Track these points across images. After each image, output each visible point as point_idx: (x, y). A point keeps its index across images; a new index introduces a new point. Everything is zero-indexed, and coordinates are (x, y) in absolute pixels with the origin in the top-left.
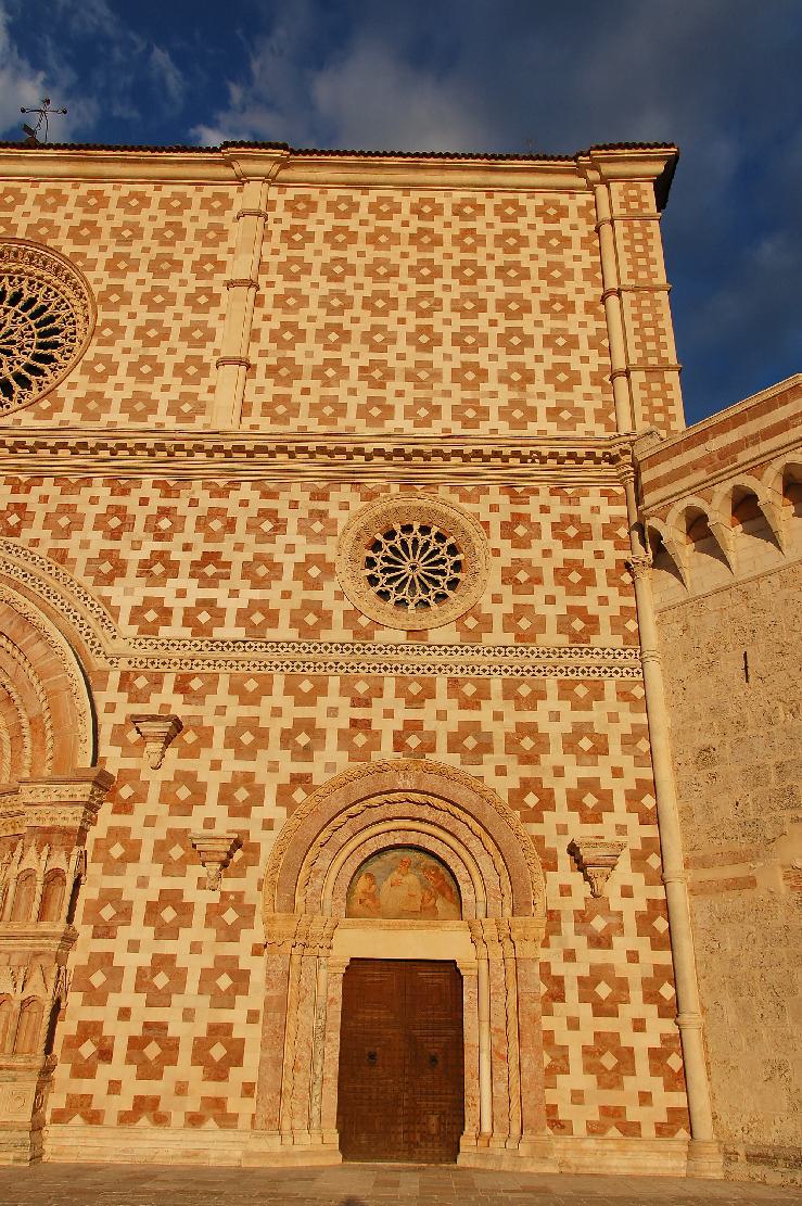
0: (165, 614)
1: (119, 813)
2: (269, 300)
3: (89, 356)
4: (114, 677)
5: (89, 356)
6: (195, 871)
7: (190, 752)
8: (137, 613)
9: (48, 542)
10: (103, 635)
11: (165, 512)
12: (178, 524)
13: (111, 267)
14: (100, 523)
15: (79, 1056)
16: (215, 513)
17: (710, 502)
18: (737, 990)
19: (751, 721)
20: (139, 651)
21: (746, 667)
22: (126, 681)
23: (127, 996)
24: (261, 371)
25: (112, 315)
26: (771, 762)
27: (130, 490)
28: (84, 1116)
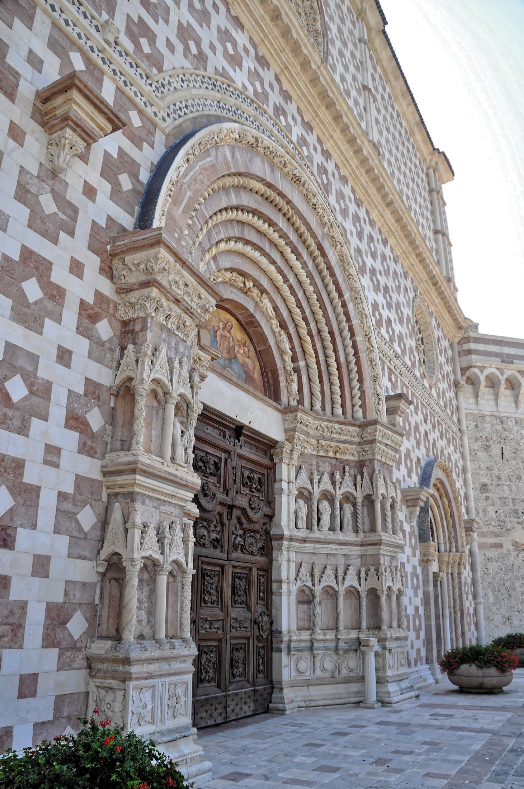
17: (502, 374)
18: (494, 590)
19: (503, 478)
21: (502, 454)
26: (510, 497)
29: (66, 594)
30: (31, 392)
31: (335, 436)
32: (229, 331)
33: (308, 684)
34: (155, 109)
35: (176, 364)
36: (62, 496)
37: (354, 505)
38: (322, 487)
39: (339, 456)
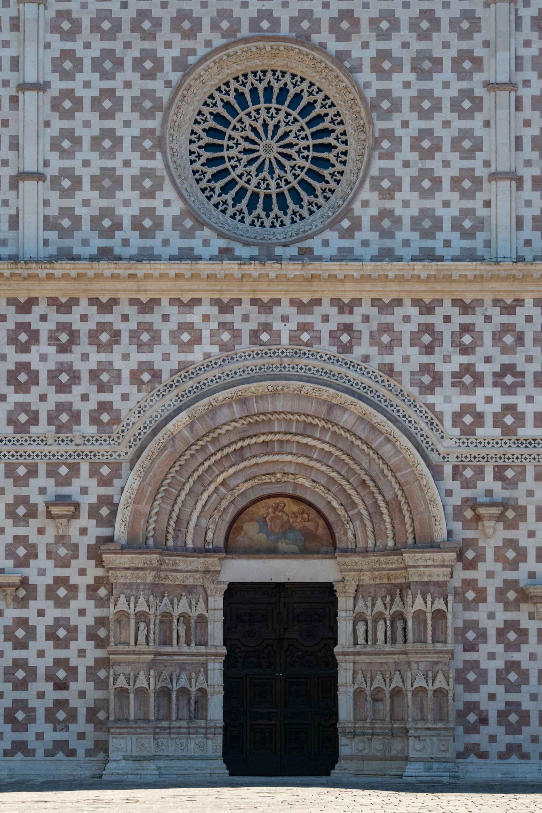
0: (479, 417)
1: (468, 569)
2: (527, 103)
3: (374, 172)
4: (448, 469)
5: (374, 172)
6: (526, 608)
7: (511, 525)
8: (457, 418)
9: (377, 359)
10: (433, 437)
11: (465, 328)
12: (478, 339)
13: (376, 67)
14: (415, 340)
15: (468, 721)
16: (507, 328)
20: (463, 450)
22: (457, 472)
23: (492, 686)
24: (528, 184)
25: (386, 125)
27: (434, 308)
28: (476, 755)
29: (95, 704)
30: (68, 632)
31: (384, 566)
32: (282, 510)
33: (364, 759)
34: (118, 453)
35: (132, 598)
36: (88, 668)
37: (405, 622)
38: (376, 609)
39: (392, 581)
